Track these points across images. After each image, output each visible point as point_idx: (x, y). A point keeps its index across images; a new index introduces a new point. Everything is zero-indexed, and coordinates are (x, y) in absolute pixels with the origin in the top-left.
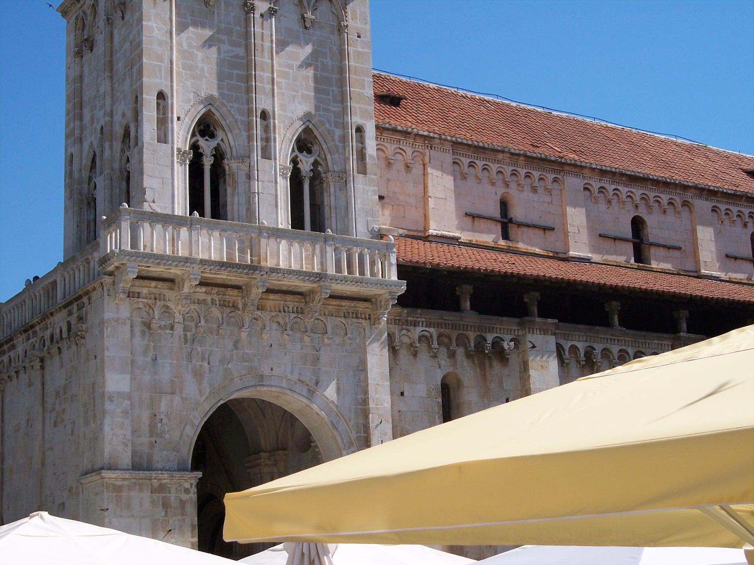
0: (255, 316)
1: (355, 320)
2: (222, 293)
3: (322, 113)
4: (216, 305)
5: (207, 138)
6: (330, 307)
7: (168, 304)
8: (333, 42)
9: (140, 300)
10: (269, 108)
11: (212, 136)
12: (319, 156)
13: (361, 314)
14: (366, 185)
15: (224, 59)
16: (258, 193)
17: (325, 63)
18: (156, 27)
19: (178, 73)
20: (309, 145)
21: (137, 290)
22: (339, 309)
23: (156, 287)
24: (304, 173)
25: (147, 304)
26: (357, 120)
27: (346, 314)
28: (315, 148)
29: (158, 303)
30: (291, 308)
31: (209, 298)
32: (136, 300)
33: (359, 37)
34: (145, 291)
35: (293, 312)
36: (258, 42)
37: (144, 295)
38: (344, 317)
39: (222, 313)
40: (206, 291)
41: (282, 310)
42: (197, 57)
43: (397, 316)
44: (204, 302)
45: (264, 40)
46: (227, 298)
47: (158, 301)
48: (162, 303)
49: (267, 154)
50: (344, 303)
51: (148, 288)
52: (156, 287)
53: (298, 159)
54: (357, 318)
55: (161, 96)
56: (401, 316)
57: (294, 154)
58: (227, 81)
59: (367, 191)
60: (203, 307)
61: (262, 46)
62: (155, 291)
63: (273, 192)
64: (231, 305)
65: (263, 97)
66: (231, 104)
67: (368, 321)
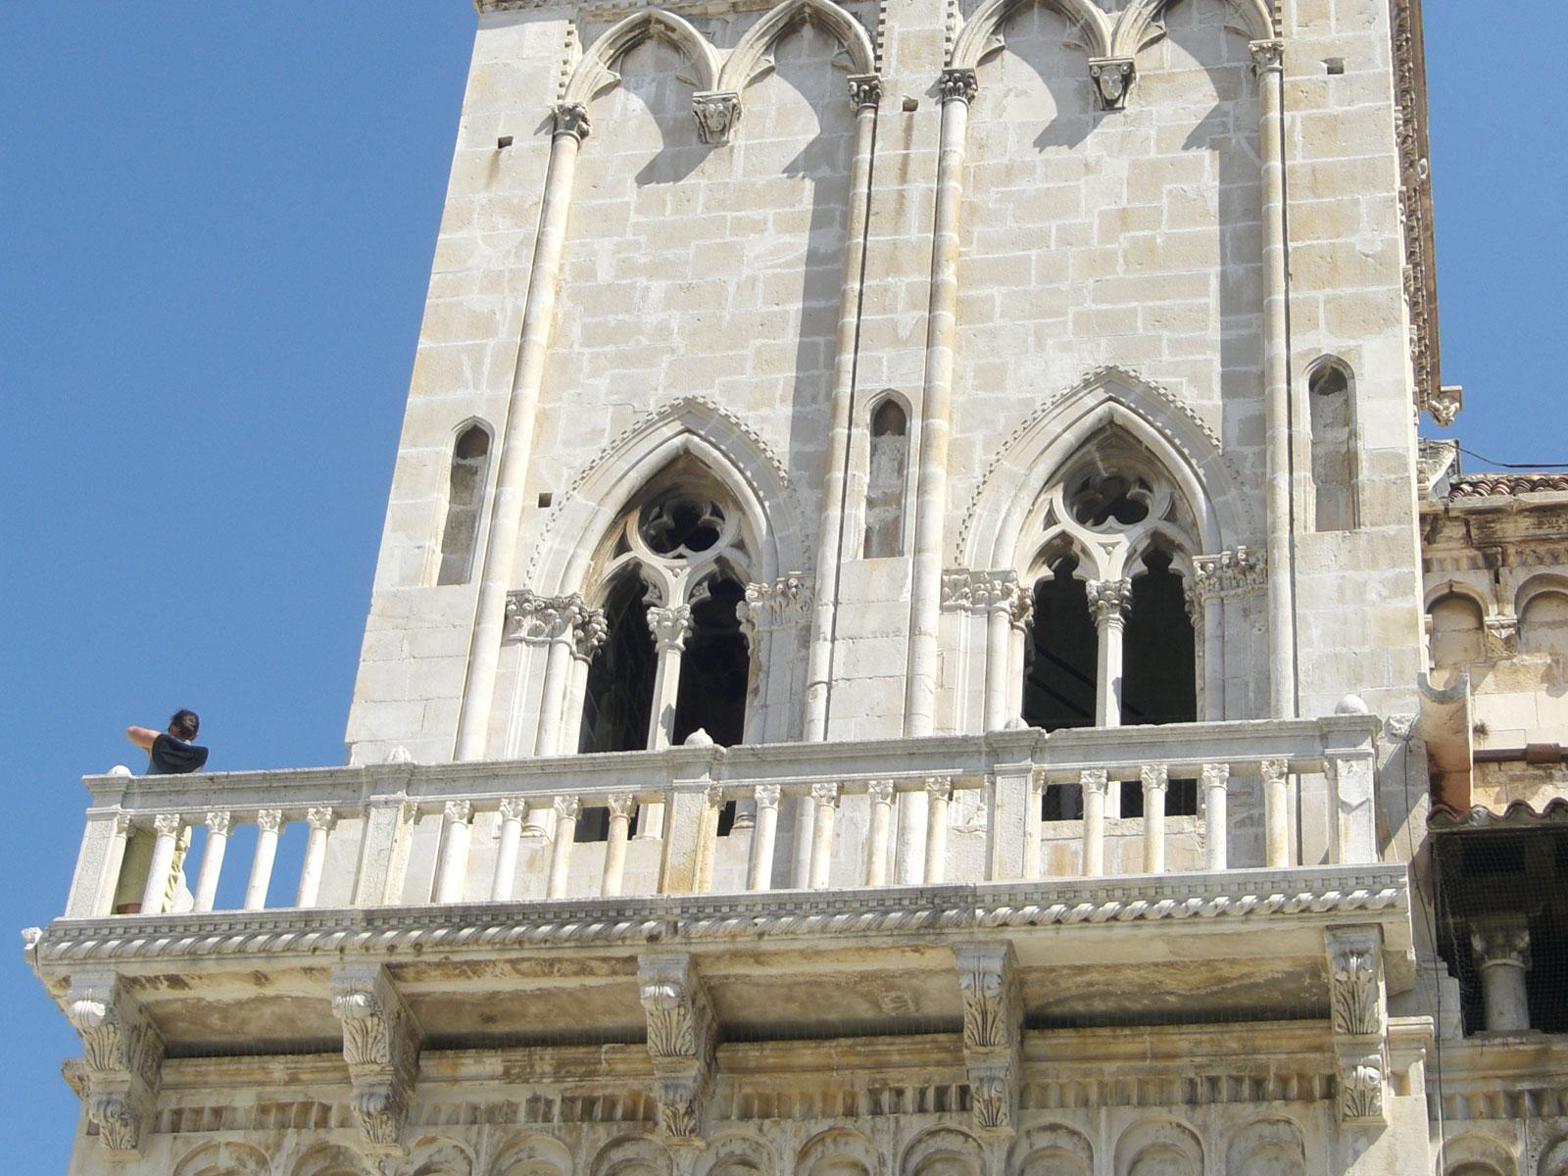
0: (738, 1148)
1: (1248, 1111)
2: (582, 1069)
3: (1166, 357)
4: (547, 1118)
5: (682, 549)
6: (1111, 1067)
7: (336, 1137)
8: (1230, 120)
9: (222, 1136)
10: (910, 386)
11: (702, 537)
12: (1171, 516)
13: (1283, 1081)
14: (1357, 567)
15: (754, 279)
16: (829, 685)
17: (1192, 195)
18: (485, 238)
19: (561, 367)
20: (1135, 490)
21: (208, 1100)
22: (1166, 1071)
23: (293, 1080)
24: (1092, 587)
25: (253, 1151)
26: (1319, 341)
27: (1203, 1090)
28: (1157, 503)
29: (291, 1138)
30: (910, 1096)
31: (520, 1095)
32: (199, 1139)
33: (1335, 69)
34: (244, 1100)
35: (922, 1109)
36: (885, 187)
37: (240, 1117)
38: (1192, 1101)
39: (573, 1149)
40: (507, 1073)
41: (863, 1104)
42: (643, 298)
43: (1520, 1078)
44: (498, 1115)
45: (910, 176)
46: (602, 1086)
47: (291, 1131)
48: (309, 1137)
49: (884, 540)
50: (1181, 1039)
51: (259, 1089)
52: (293, 1080)
53: (1076, 549)
54: (1259, 1094)
55: (472, 441)
56: (1544, 1075)
57: (1054, 530)
58: (758, 342)
59: (1361, 588)
60: (488, 1138)
61: (901, 195)
62: (284, 1095)
63: (902, 670)
64: (619, 1112)
65: (885, 354)
66: (764, 411)
67: (1321, 1106)
